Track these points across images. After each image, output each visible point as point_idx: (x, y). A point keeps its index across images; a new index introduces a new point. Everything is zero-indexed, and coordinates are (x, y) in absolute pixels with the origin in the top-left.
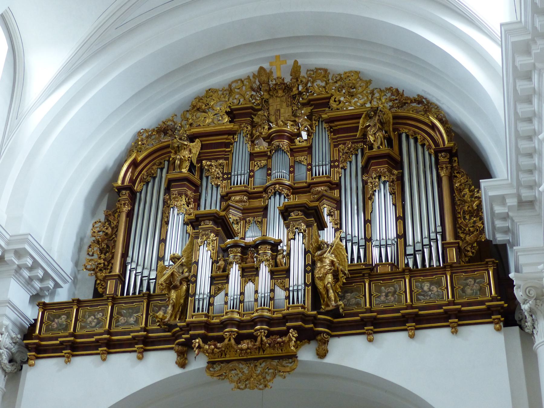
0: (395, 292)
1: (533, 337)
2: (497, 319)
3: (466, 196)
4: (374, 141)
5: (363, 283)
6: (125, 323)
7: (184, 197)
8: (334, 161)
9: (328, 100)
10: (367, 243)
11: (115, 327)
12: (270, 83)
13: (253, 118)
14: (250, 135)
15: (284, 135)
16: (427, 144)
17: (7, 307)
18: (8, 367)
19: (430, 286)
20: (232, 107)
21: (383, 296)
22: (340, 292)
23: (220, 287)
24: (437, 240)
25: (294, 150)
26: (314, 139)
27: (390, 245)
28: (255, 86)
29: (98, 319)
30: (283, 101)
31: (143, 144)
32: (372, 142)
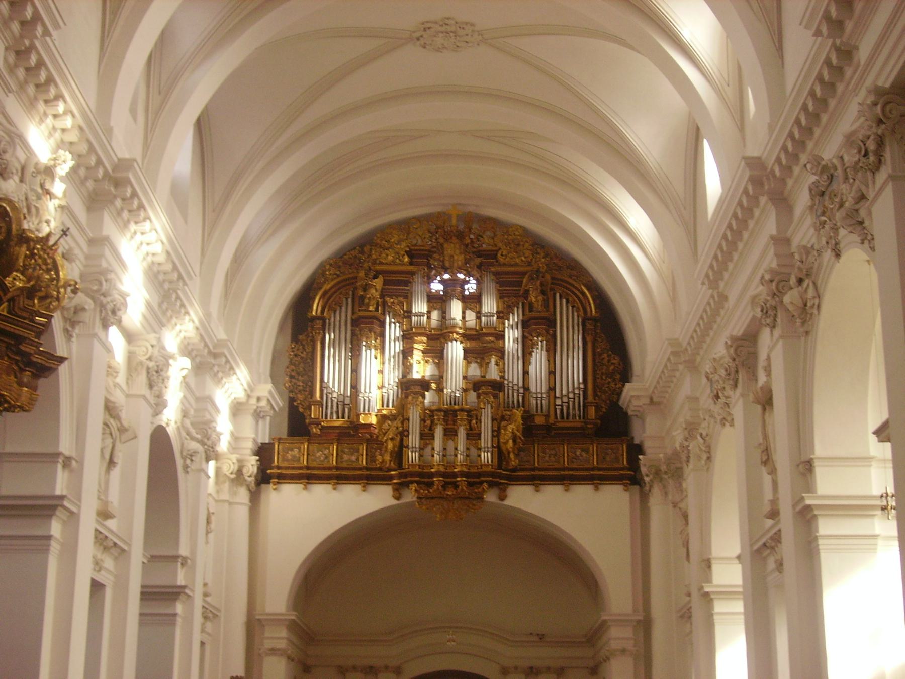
0: (556, 455)
7: (373, 334)
9: (495, 253)
13: (429, 260)
16: (576, 305)
24: (579, 394)
29: (325, 454)
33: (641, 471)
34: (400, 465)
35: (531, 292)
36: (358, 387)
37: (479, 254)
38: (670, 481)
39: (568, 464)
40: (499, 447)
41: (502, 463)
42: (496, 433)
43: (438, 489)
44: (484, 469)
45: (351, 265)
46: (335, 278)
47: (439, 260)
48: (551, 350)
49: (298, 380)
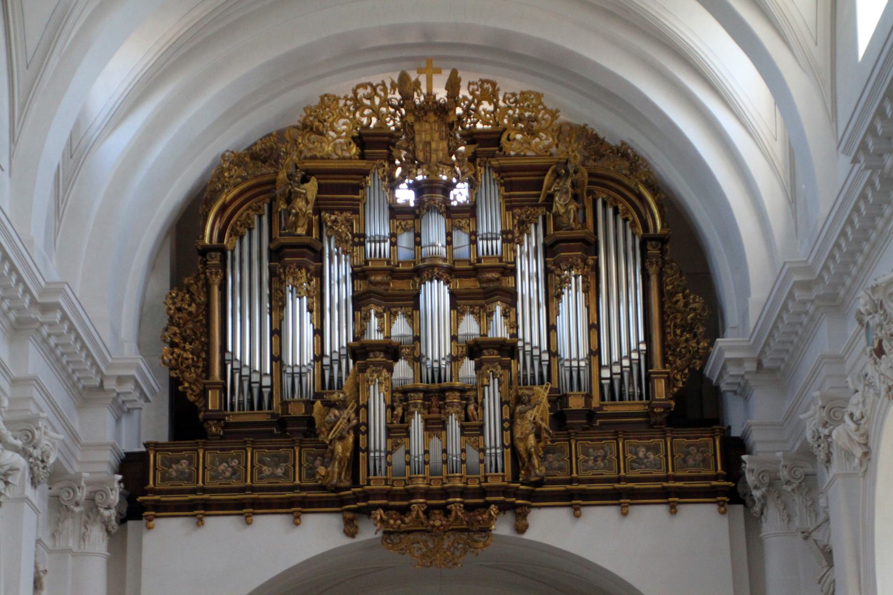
0: (604, 457)
1: (759, 522)
3: (679, 303)
4: (564, 213)
5: (567, 443)
7: (304, 271)
9: (497, 136)
10: (552, 358)
11: (258, 479)
12: (416, 96)
13: (392, 151)
14: (388, 177)
15: (439, 188)
16: (631, 218)
18: (115, 527)
19: (646, 452)
21: (591, 460)
23: (399, 442)
24: (639, 360)
26: (479, 194)
27: (583, 368)
28: (395, 102)
29: (232, 467)
31: (232, 177)
32: (561, 213)
33: (745, 482)
34: (355, 481)
35: (557, 198)
36: (284, 358)
37: (472, 137)
38: (796, 498)
39: (625, 471)
40: (513, 447)
41: (519, 473)
42: (509, 424)
43: (418, 517)
44: (492, 482)
45: (264, 162)
46: (239, 184)
47: (407, 149)
48: (592, 290)
49: (184, 349)
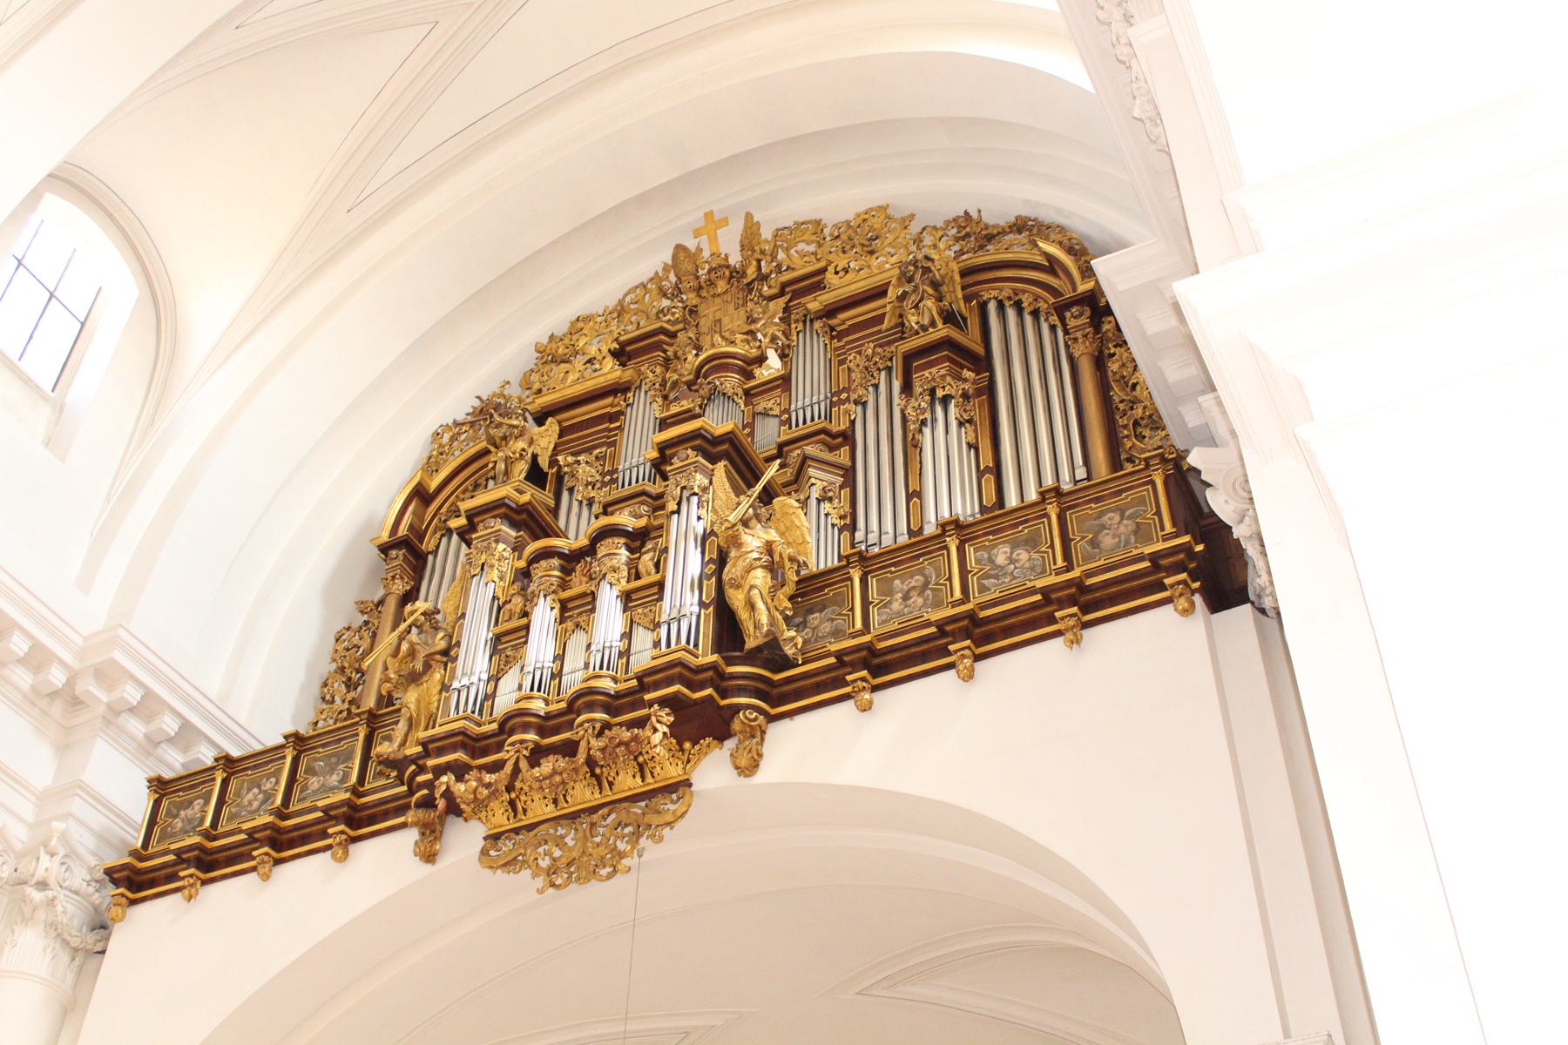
0: (925, 586)
2: (1179, 583)
6: (319, 789)
8: (839, 393)
17: (77, 798)
19: (1012, 553)
20: (622, 339)
21: (897, 600)
22: (789, 609)
25: (752, 392)
30: (727, 302)
